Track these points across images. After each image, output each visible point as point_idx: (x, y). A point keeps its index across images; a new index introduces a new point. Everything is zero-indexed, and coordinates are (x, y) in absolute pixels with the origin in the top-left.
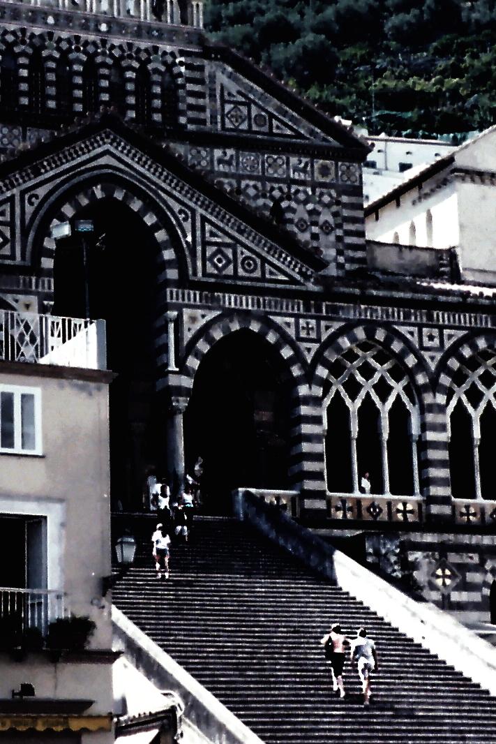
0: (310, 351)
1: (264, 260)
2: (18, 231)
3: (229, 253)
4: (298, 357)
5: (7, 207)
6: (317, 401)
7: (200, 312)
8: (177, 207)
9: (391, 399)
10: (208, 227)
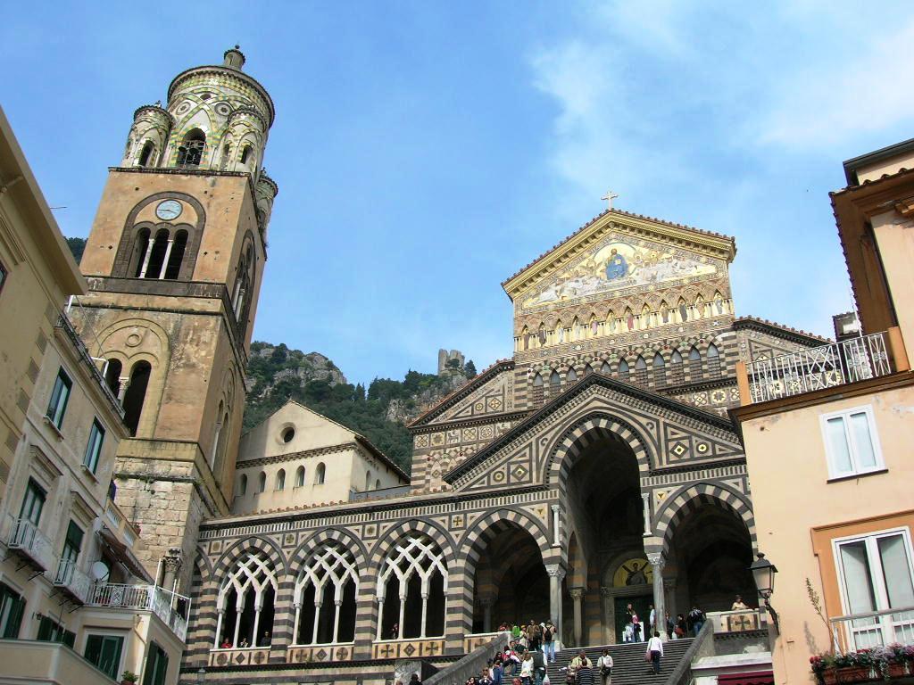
1: (714, 443)
2: (534, 464)
5: (527, 450)
8: (644, 421)
10: (670, 430)
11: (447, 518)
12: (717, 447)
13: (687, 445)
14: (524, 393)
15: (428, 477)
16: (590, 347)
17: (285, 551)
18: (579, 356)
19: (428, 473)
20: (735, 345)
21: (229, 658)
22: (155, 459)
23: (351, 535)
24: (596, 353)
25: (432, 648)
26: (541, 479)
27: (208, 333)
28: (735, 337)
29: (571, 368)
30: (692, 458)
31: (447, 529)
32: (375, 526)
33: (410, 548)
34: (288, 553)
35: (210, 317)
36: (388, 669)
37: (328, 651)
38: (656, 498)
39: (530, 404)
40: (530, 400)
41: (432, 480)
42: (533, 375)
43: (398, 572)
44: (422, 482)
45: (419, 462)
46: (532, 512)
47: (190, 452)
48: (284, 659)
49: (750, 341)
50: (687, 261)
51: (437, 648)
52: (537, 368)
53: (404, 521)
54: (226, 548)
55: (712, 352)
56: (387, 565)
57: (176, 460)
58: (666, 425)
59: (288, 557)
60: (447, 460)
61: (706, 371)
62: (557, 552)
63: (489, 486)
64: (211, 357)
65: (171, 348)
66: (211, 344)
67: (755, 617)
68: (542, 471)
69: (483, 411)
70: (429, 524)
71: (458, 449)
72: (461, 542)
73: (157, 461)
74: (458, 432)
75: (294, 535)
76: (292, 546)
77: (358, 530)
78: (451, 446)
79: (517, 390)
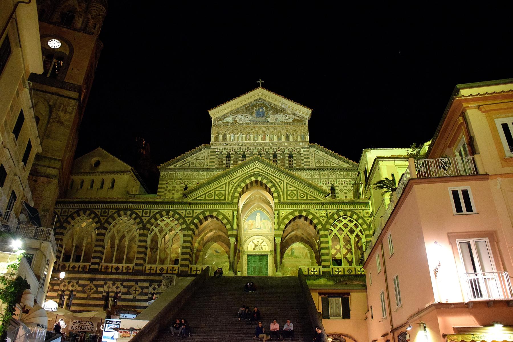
0: (324, 220)
1: (307, 194)
2: (227, 192)
3: (295, 192)
4: (320, 222)
5: (224, 186)
6: (326, 236)
7: (284, 211)
8: (278, 181)
9: (355, 234)
10: (288, 185)
11: (184, 211)
12: (308, 196)
13: (296, 193)
14: (214, 160)
15: (166, 192)
16: (245, 145)
17: (101, 218)
18: (240, 148)
19: (166, 190)
20: (308, 155)
21: (67, 267)
22: (38, 165)
23: (136, 214)
24: (248, 148)
25: (173, 270)
26: (230, 199)
27: (71, 108)
28: (309, 151)
29: (236, 152)
30: (297, 200)
31: (184, 216)
32: (149, 211)
33: (165, 223)
34: (103, 219)
35: (73, 101)
36: (151, 278)
37: (121, 268)
38: (281, 214)
39: (216, 166)
40: (216, 164)
41: (168, 193)
42: (219, 153)
43: (158, 233)
44: (163, 194)
45: (161, 184)
46: (225, 214)
47: (58, 165)
48: (98, 269)
49: (315, 154)
50: (291, 116)
51: (175, 270)
52: (221, 151)
53: (164, 210)
54: (70, 213)
55: (299, 156)
56: (153, 230)
57: (49, 167)
58: (287, 184)
59: (103, 221)
60: (176, 185)
61: (295, 164)
62: (235, 232)
63: (205, 199)
64: (72, 120)
65: (51, 112)
66: (72, 113)
67: (320, 269)
68: (230, 196)
69: (194, 166)
70: (175, 212)
71: (181, 181)
72: (190, 222)
73: (39, 167)
74: (181, 173)
75: (107, 211)
76: (106, 216)
77: (140, 212)
78: (178, 179)
79: (211, 159)
